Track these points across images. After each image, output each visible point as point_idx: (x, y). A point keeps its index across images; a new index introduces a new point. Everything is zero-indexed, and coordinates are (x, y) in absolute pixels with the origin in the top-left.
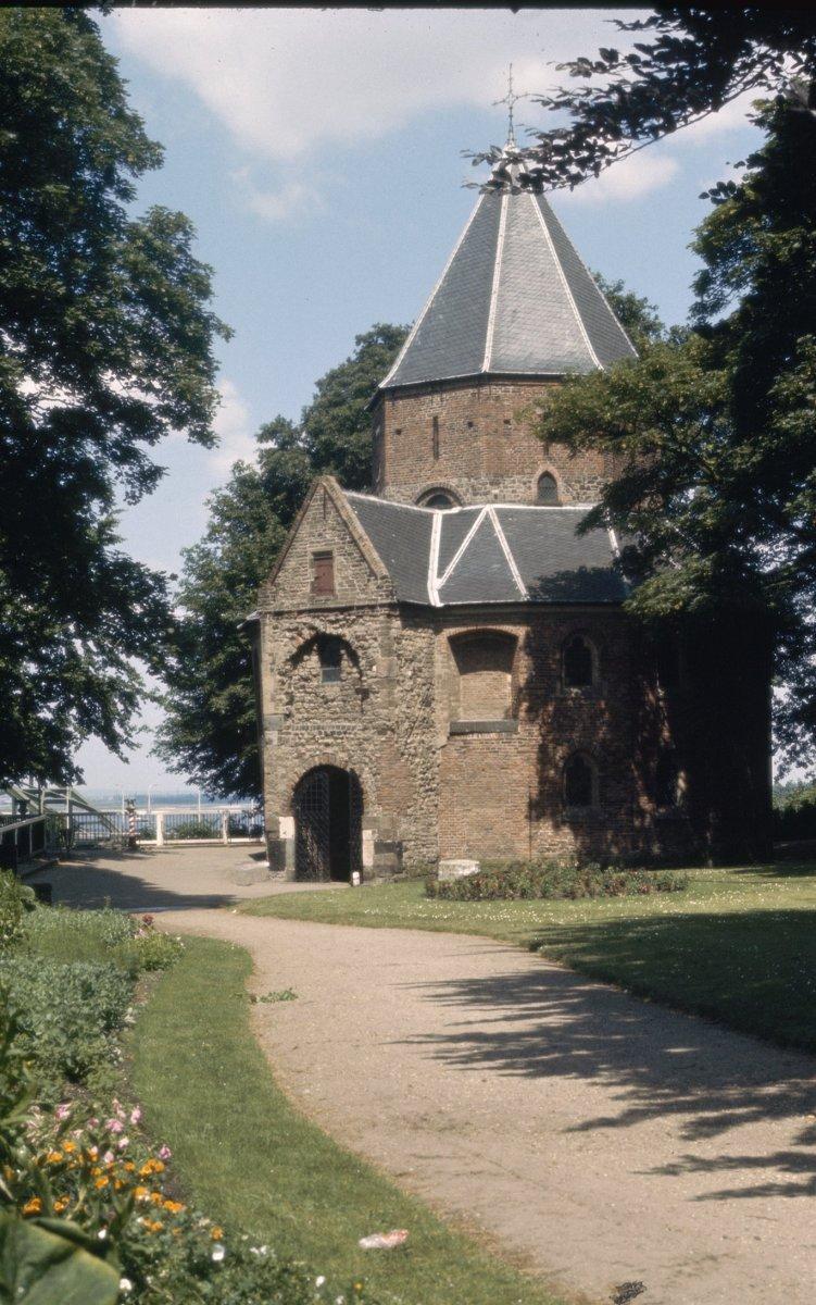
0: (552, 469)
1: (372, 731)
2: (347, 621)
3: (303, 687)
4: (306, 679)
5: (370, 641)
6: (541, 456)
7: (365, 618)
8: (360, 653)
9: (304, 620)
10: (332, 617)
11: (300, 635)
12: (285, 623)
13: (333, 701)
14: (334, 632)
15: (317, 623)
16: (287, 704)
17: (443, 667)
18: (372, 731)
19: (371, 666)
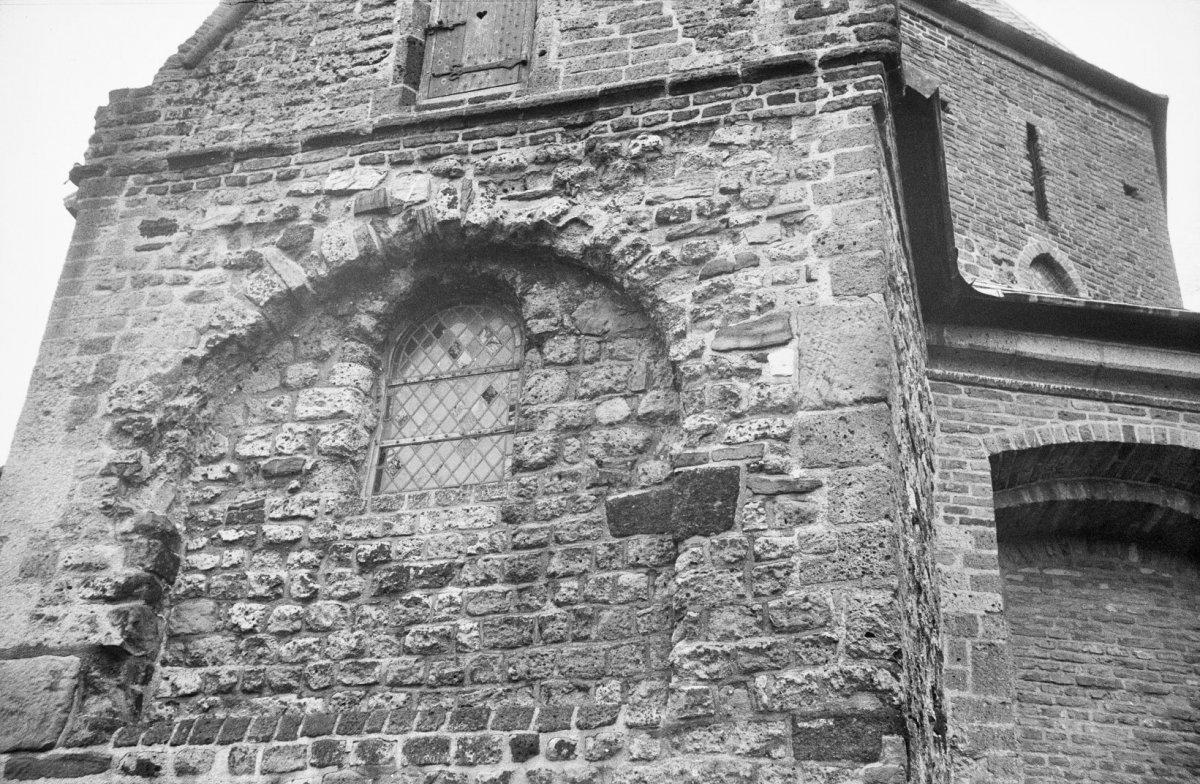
0: (1061, 257)
1: (749, 737)
2: (603, 160)
3: (252, 514)
4: (287, 475)
5: (754, 233)
6: (1032, 215)
7: (722, 134)
8: (679, 295)
9: (336, 181)
10: (512, 152)
11: (294, 249)
12: (216, 207)
13: (442, 576)
14: (516, 214)
15: (413, 186)
16: (125, 592)
17: (978, 583)
18: (749, 737)
19: (760, 352)
